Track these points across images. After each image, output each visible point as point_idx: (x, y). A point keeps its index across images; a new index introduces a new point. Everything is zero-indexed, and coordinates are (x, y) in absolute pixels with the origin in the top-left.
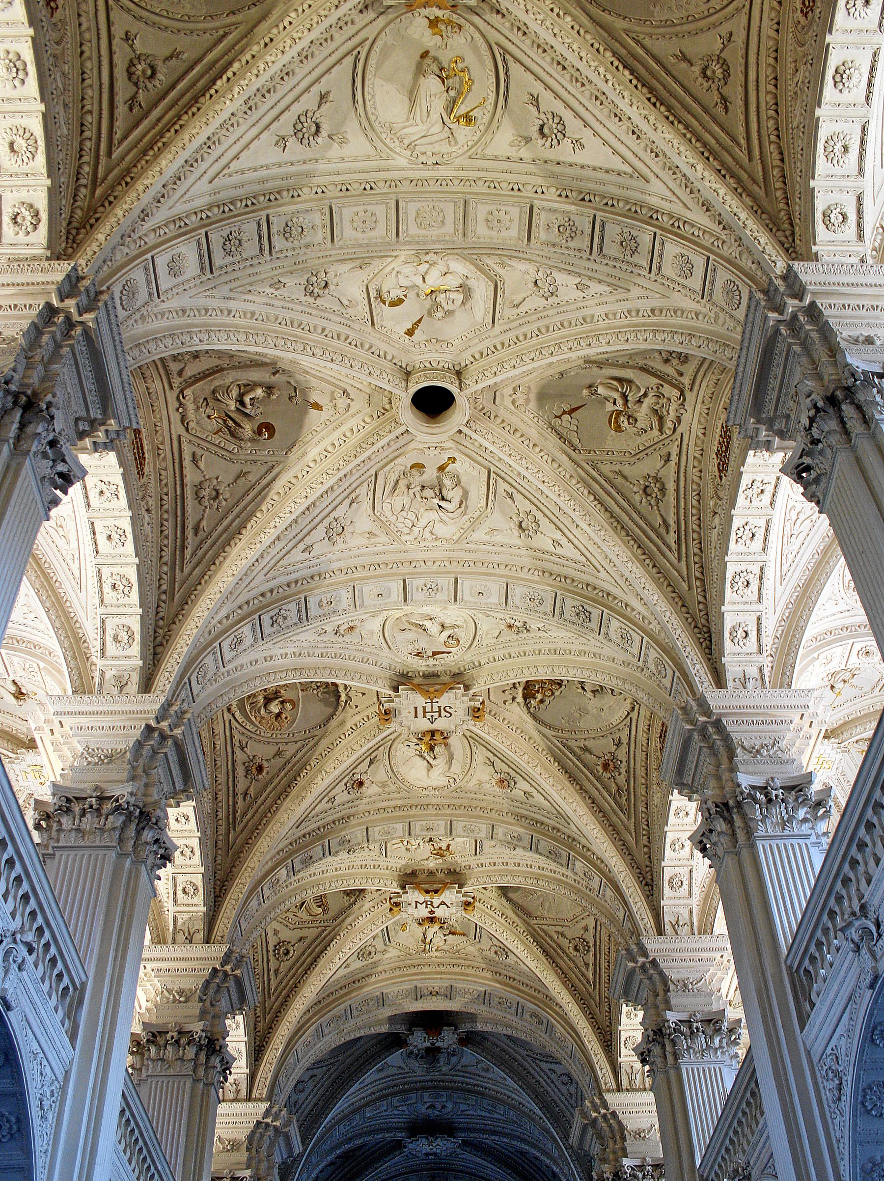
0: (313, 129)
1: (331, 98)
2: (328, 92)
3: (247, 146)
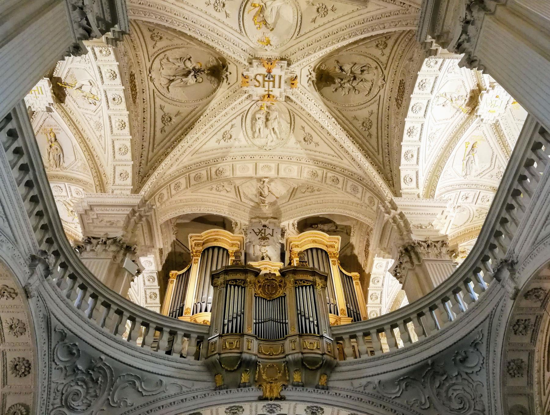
0: (320, 10)
1: (311, 20)
2: (312, 22)
3: (348, 14)
